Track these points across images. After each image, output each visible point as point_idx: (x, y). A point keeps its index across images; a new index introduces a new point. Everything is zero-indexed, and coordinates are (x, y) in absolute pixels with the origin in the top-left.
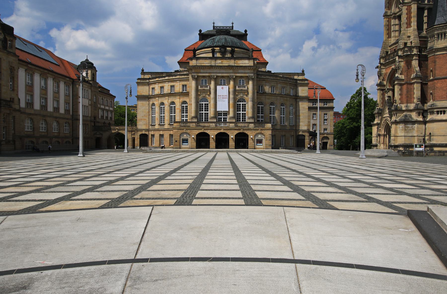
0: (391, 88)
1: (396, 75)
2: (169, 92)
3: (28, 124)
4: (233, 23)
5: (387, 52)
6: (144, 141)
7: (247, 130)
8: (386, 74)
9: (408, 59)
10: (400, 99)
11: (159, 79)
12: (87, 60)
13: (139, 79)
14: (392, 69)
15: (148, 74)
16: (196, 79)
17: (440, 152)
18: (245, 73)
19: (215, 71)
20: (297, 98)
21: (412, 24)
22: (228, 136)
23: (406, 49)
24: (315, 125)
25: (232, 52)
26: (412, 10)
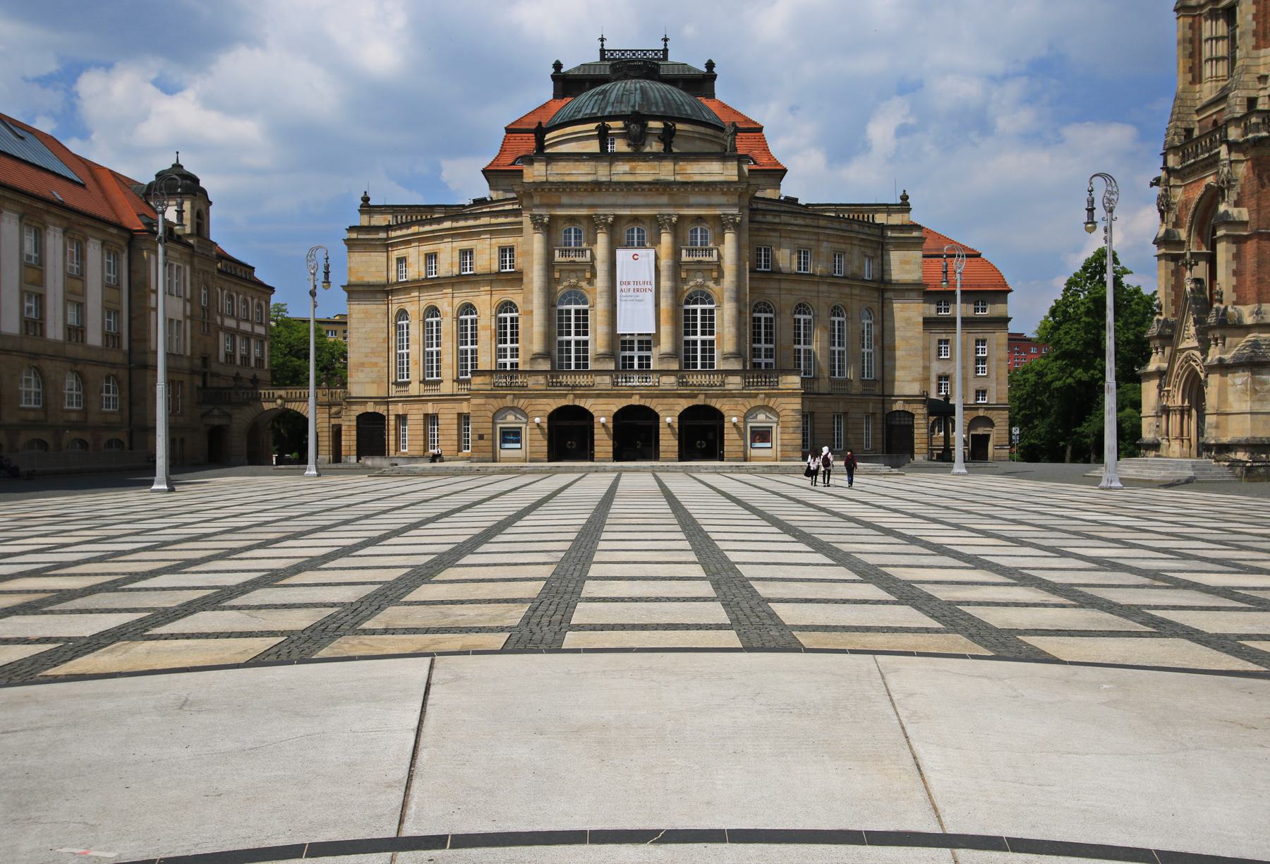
0: (1204, 250)
1: (1222, 208)
2: (456, 271)
3: (29, 388)
4: (666, 40)
5: (1189, 131)
6: (373, 436)
7: (717, 396)
8: (1185, 204)
10: (1235, 289)
11: (422, 229)
12: (177, 166)
13: (351, 229)
14: (1208, 187)
15: (382, 213)
16: (548, 227)
18: (710, 206)
19: (610, 200)
20: (884, 289)
22: (656, 417)
23: (1254, 120)
24: (947, 378)
25: (667, 136)
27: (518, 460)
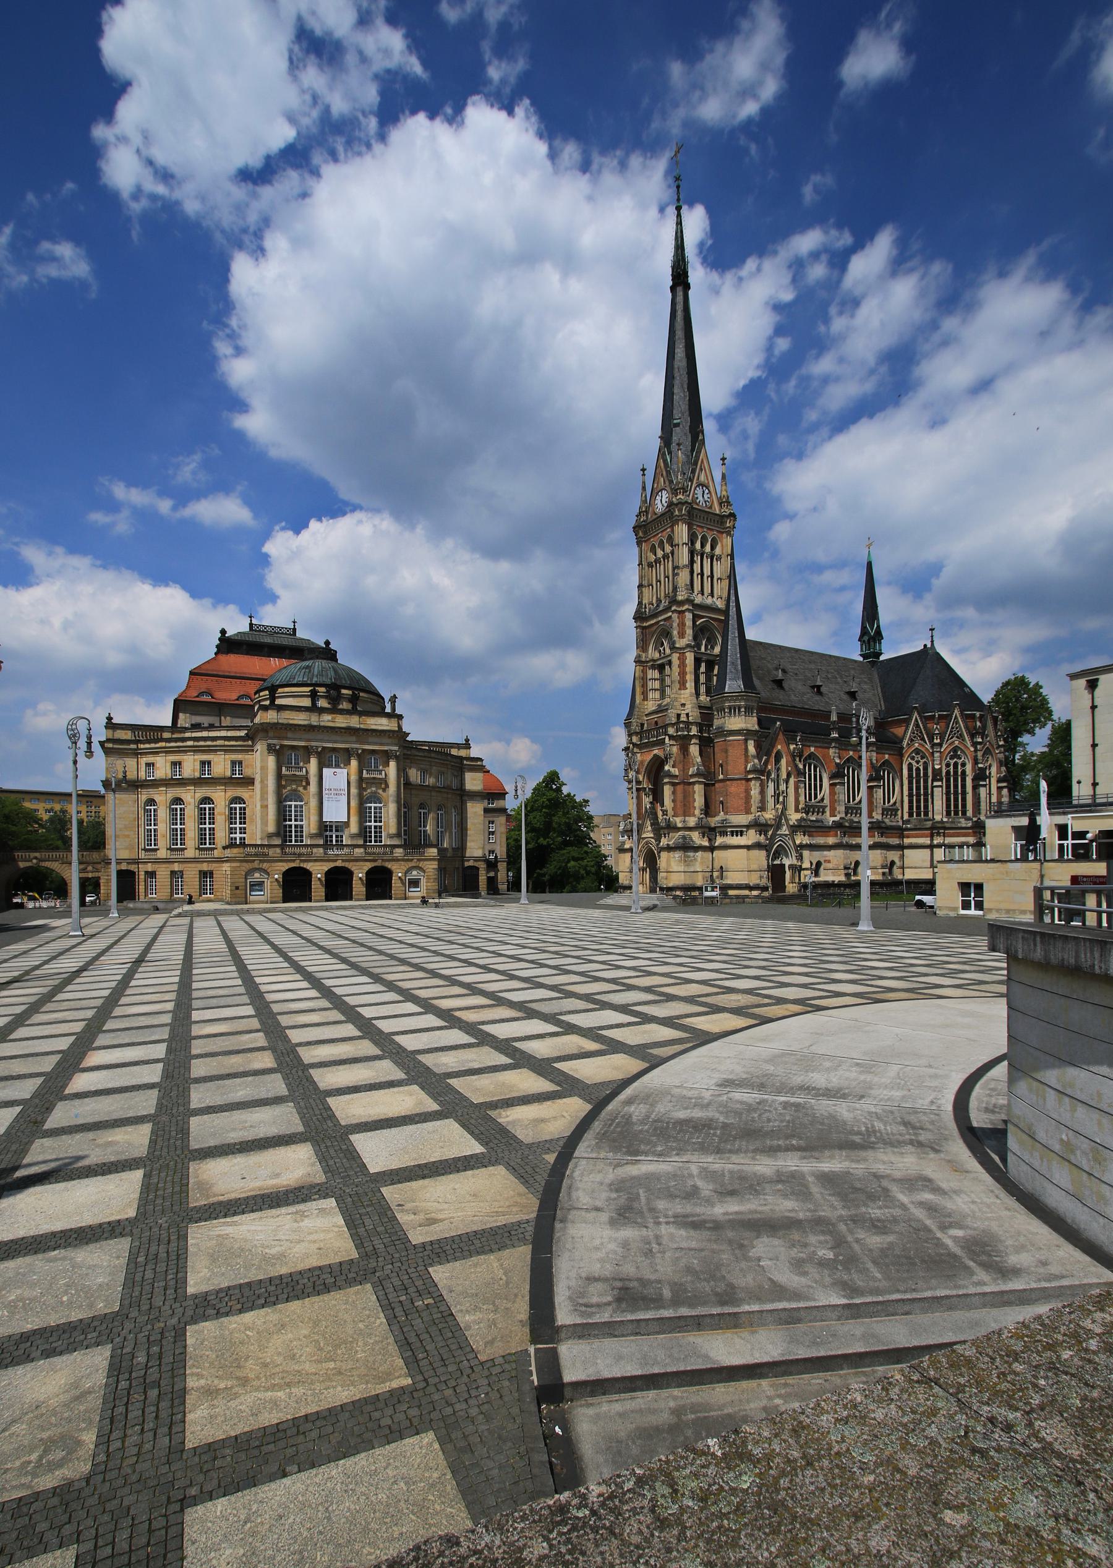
1: (667, 768)
5: (642, 725)
8: (642, 762)
9: (683, 742)
16: (280, 753)
17: (737, 897)
18: (381, 744)
19: (320, 737)
20: (463, 795)
21: (688, 685)
25: (353, 700)
26: (687, 662)
27: (262, 902)
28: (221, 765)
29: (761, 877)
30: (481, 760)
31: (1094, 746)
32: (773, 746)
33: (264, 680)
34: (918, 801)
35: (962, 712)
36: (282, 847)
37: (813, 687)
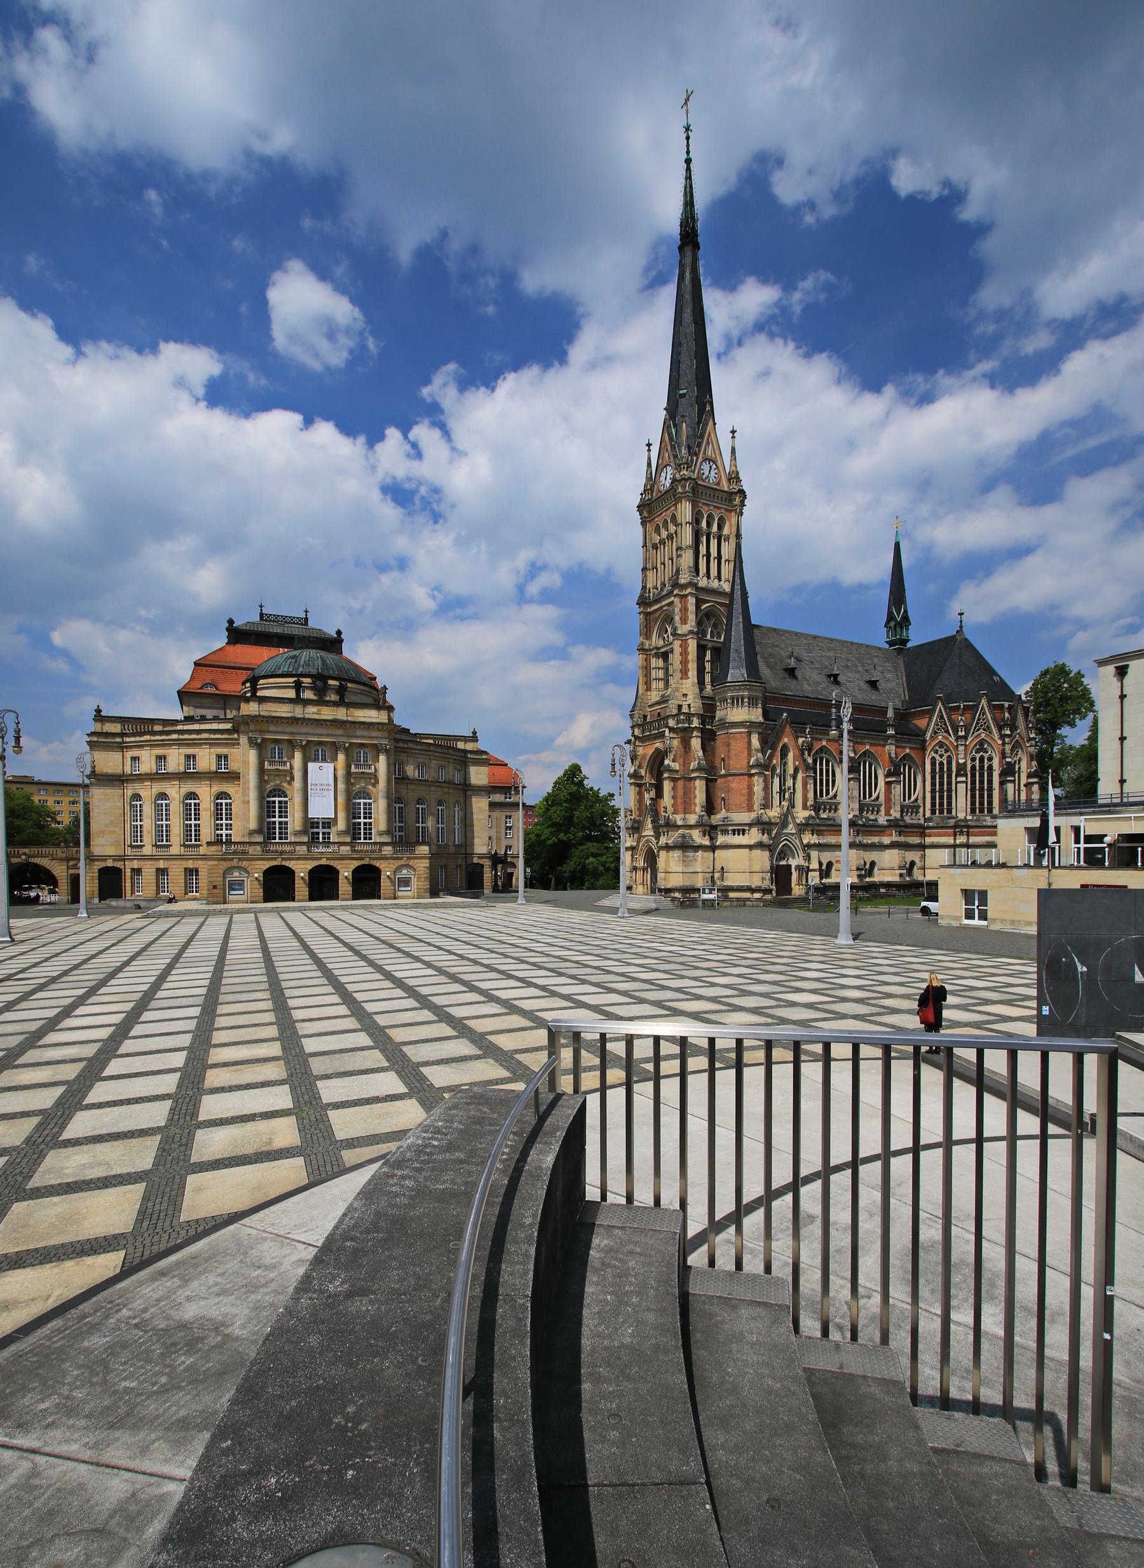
1: (666, 762)
5: (645, 717)
6: (111, 883)
8: (644, 756)
9: (685, 734)
11: (153, 738)
13: (93, 734)
15: (112, 722)
16: (260, 746)
17: (738, 899)
19: (304, 730)
20: (466, 789)
21: (690, 674)
22: (337, 872)
25: (341, 691)
26: (690, 649)
27: (242, 902)
28: (206, 759)
29: (763, 879)
30: (485, 753)
31: (1122, 739)
32: (779, 738)
33: (252, 669)
34: (941, 798)
35: (989, 702)
36: (264, 844)
37: (829, 676)
